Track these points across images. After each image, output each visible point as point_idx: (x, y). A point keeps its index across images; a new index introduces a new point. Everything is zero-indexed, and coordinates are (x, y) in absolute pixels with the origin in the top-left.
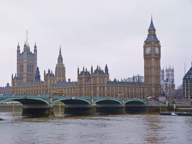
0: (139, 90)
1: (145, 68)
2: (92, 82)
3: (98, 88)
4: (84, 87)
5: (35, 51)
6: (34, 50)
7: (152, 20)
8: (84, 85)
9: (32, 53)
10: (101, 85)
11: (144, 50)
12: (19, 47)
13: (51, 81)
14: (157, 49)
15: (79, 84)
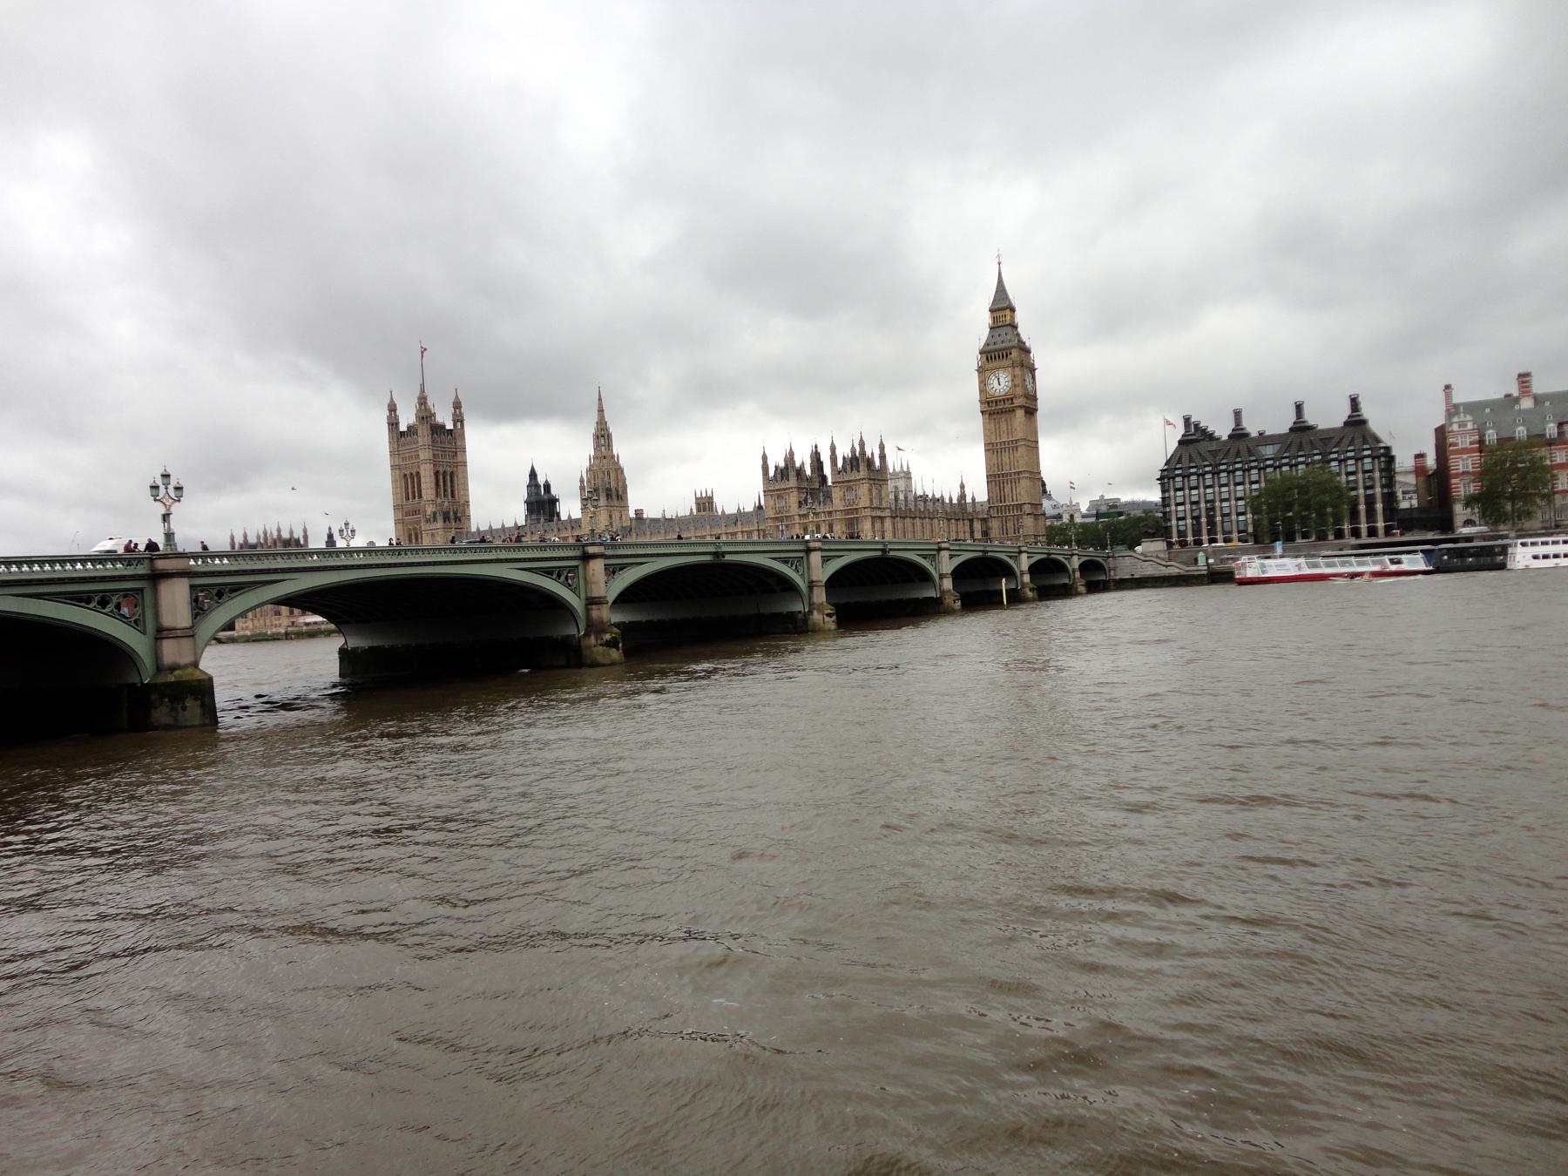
0: (967, 529)
1: (991, 448)
2: (838, 501)
3: (867, 525)
4: (797, 526)
5: (459, 419)
6: (454, 415)
7: (1000, 274)
8: (797, 518)
9: (444, 426)
10: (874, 514)
11: (980, 382)
12: (392, 408)
13: (611, 516)
14: (1029, 379)
15: (771, 514)
